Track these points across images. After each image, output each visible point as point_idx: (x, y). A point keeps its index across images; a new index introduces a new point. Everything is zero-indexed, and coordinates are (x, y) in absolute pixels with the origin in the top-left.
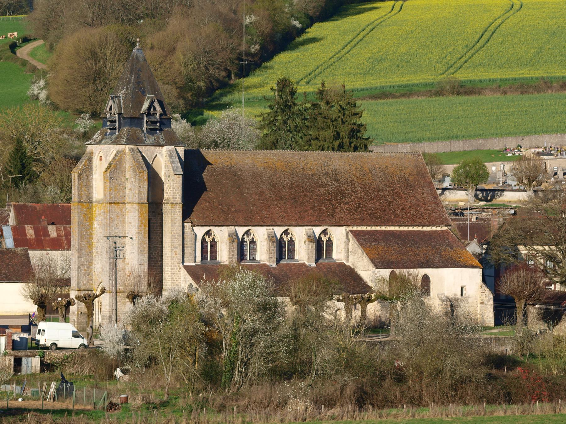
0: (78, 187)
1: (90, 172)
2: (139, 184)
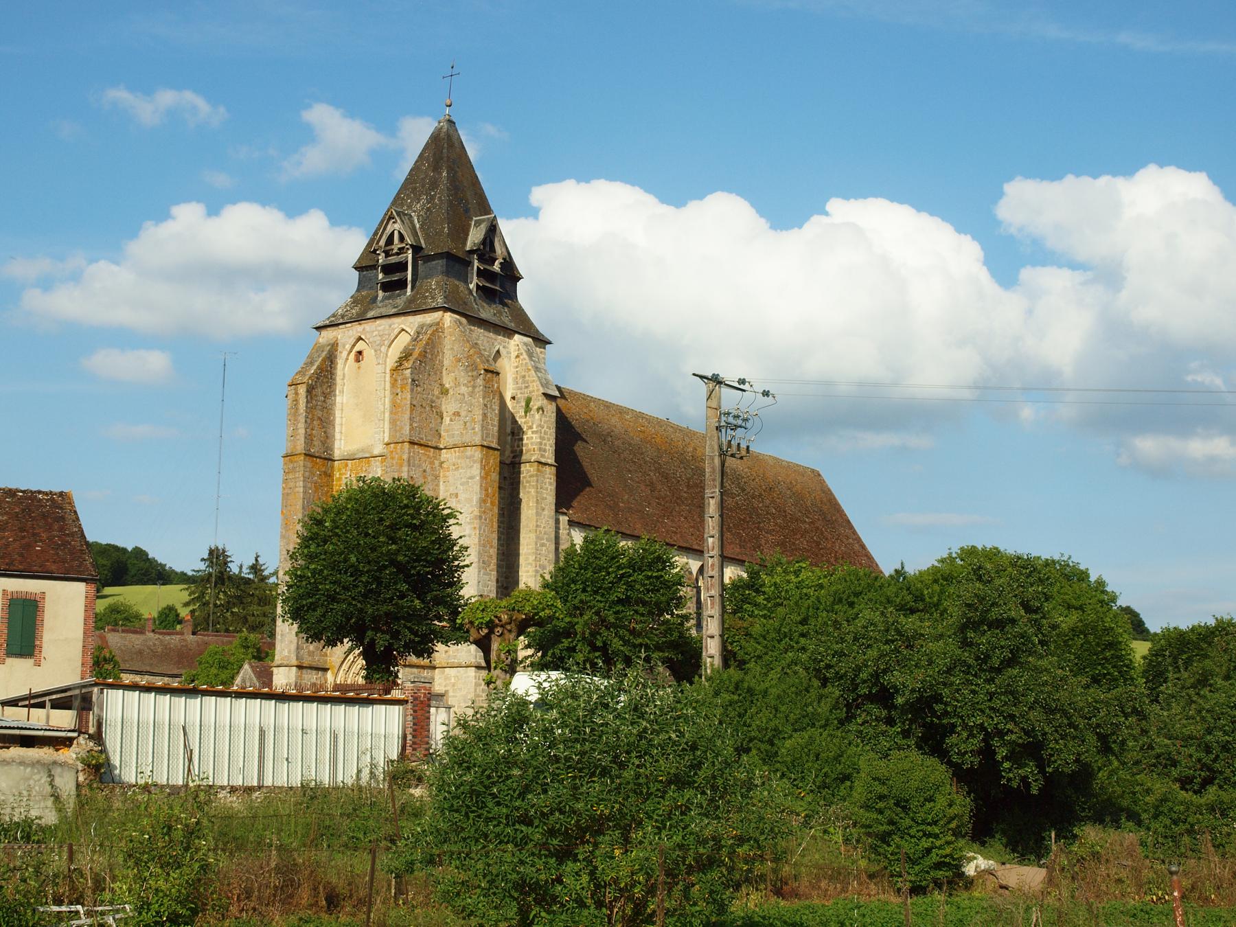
0: (307, 417)
2: (484, 398)
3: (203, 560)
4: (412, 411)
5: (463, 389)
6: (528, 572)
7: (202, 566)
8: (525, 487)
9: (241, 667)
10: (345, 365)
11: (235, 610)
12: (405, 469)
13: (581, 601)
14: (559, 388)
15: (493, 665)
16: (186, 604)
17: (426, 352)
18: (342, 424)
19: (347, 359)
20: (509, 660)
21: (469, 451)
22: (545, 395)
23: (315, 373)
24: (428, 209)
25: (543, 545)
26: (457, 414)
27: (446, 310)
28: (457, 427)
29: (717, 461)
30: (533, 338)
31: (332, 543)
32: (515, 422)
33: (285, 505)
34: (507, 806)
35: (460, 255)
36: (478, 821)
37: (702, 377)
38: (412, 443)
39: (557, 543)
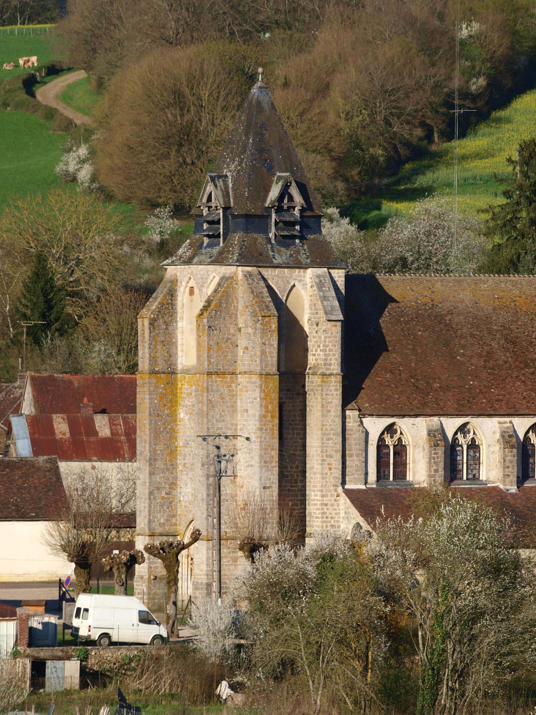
2: (262, 338)
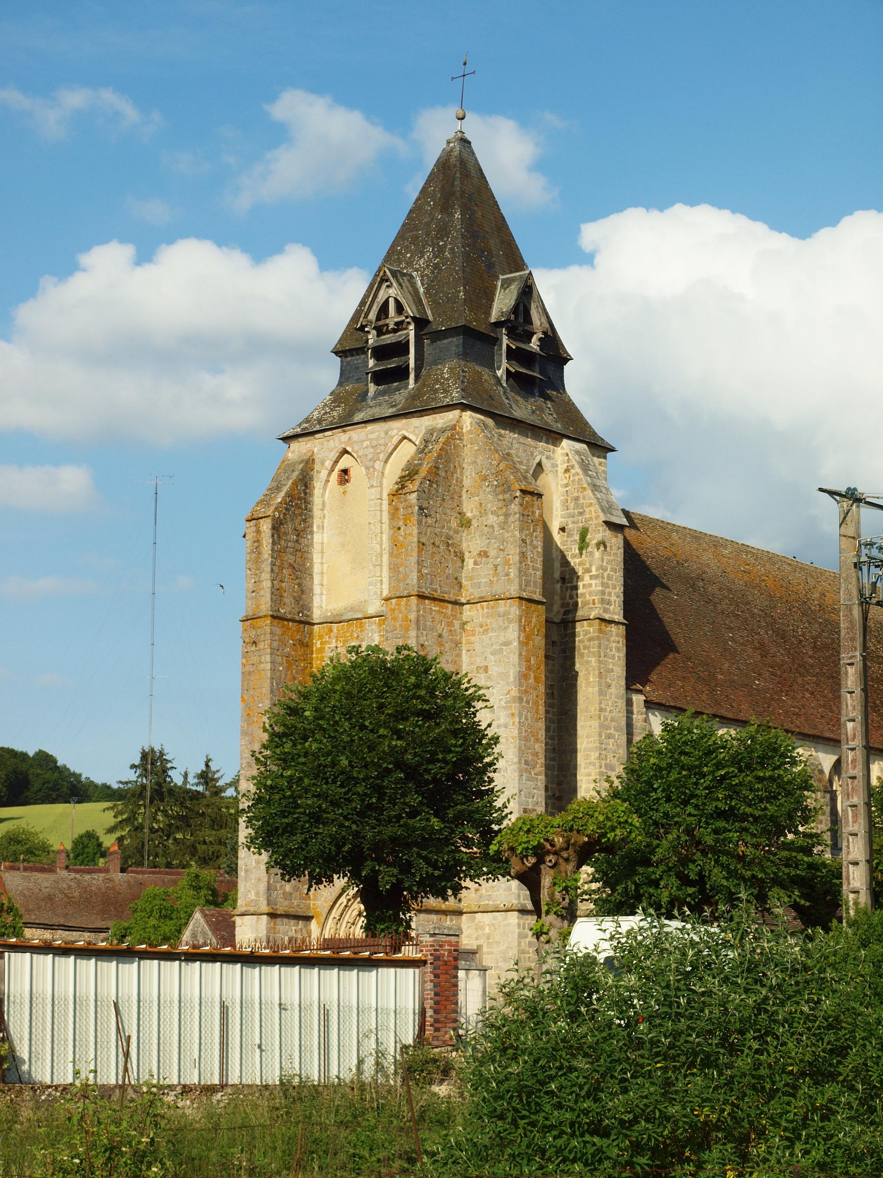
1: (305, 521)
2: (521, 530)
3: (133, 766)
4: (420, 551)
5: (492, 519)
6: (589, 775)
7: (132, 776)
8: (582, 655)
9: (190, 916)
10: (325, 489)
11: (179, 836)
12: (413, 633)
13: (666, 815)
14: (626, 514)
15: (544, 908)
16: (111, 830)
17: (438, 468)
18: (322, 573)
19: (327, 481)
20: (567, 900)
21: (502, 606)
22: (608, 524)
23: (284, 499)
24: (436, 266)
25: (609, 736)
26: (484, 554)
27: (464, 407)
28: (484, 573)
29: (856, 612)
30: (589, 444)
31: (315, 740)
32: (565, 563)
33: (245, 689)
34: (572, 1110)
35: (482, 328)
36: (531, 1132)
37: (832, 493)
38: (421, 597)
39: (630, 733)
